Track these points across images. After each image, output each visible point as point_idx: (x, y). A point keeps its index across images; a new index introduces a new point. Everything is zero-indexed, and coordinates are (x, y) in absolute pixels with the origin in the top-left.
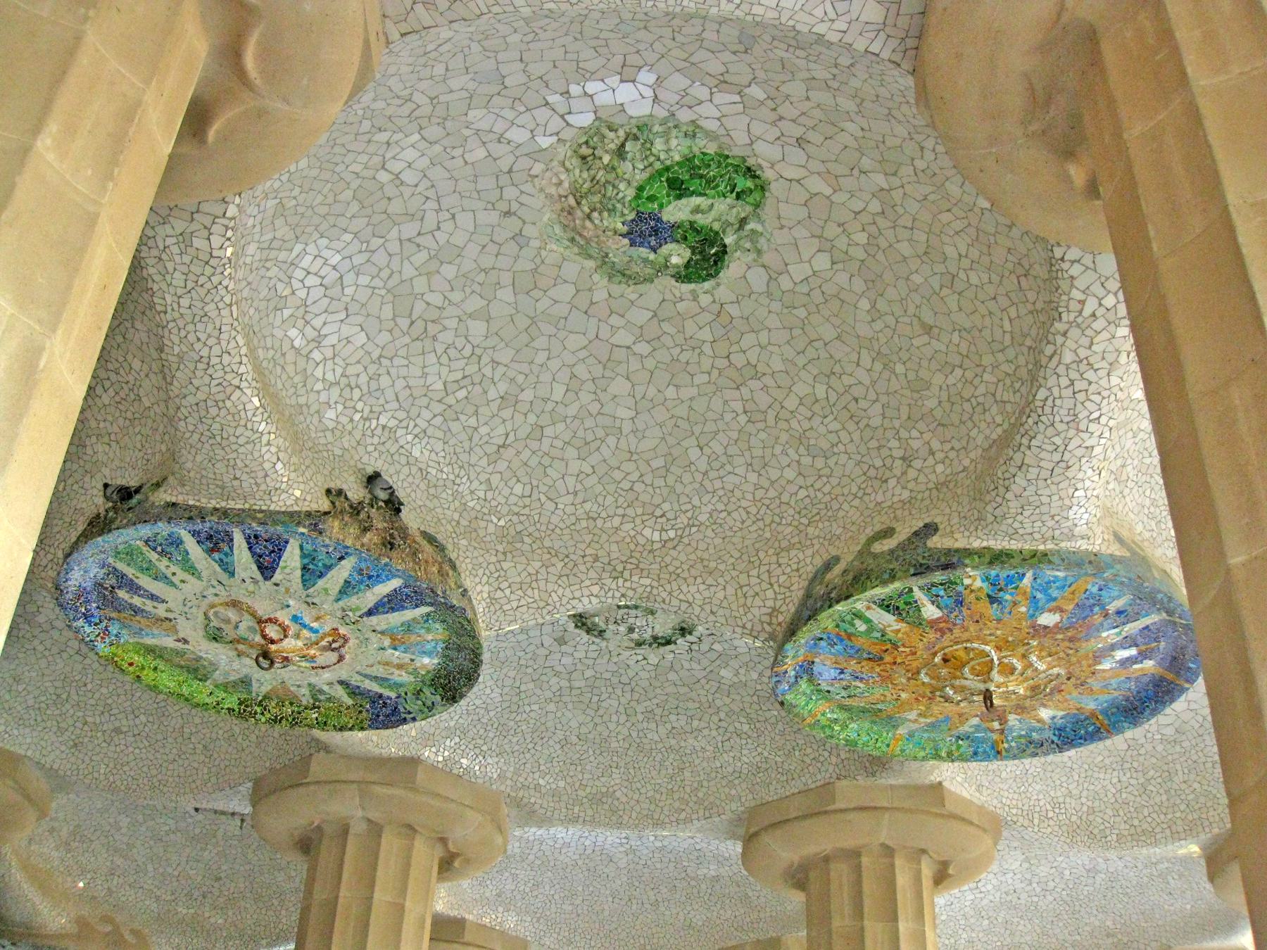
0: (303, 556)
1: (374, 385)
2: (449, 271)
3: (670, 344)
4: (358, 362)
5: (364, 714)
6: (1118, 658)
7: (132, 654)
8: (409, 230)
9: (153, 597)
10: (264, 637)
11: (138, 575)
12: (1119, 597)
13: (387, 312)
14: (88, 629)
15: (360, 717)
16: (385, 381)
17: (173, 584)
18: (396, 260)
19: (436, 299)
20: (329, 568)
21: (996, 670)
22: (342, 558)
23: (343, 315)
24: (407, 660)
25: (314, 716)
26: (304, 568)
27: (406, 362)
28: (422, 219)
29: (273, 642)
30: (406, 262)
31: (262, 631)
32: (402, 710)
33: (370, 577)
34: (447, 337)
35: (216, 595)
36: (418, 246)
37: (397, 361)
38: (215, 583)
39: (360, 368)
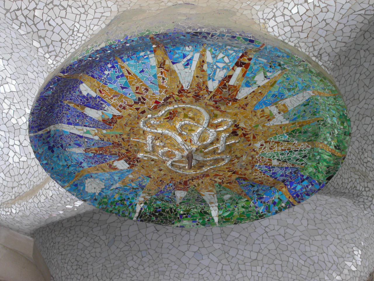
1: (350, 241)
2: (290, 221)
4: (342, 247)
6: (100, 112)
8: (280, 239)
12: (75, 153)
13: (318, 238)
16: (347, 237)
18: (294, 239)
19: (305, 222)
21: (174, 159)
23: (324, 254)
27: (336, 230)
28: (273, 236)
30: (294, 235)
34: (318, 216)
36: (285, 233)
37: (338, 233)
39: (345, 247)
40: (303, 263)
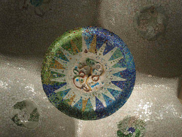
0: (118, 91)
3: (108, 131)
5: (48, 83)
7: (77, 34)
9: (105, 53)
10: (94, 76)
11: (113, 53)
14: (92, 30)
15: (47, 82)
17: (110, 60)
20: (113, 95)
22: (115, 98)
24: (74, 100)
25: (46, 70)
26: (114, 90)
29: (92, 77)
31: (96, 76)
32: (51, 94)
33: (108, 102)
35: (106, 68)
38: (111, 70)
40: (142, 93)
